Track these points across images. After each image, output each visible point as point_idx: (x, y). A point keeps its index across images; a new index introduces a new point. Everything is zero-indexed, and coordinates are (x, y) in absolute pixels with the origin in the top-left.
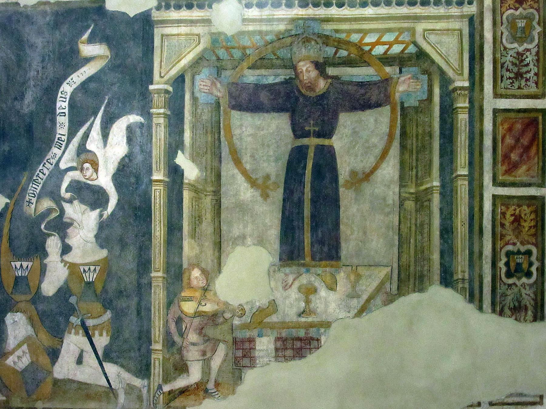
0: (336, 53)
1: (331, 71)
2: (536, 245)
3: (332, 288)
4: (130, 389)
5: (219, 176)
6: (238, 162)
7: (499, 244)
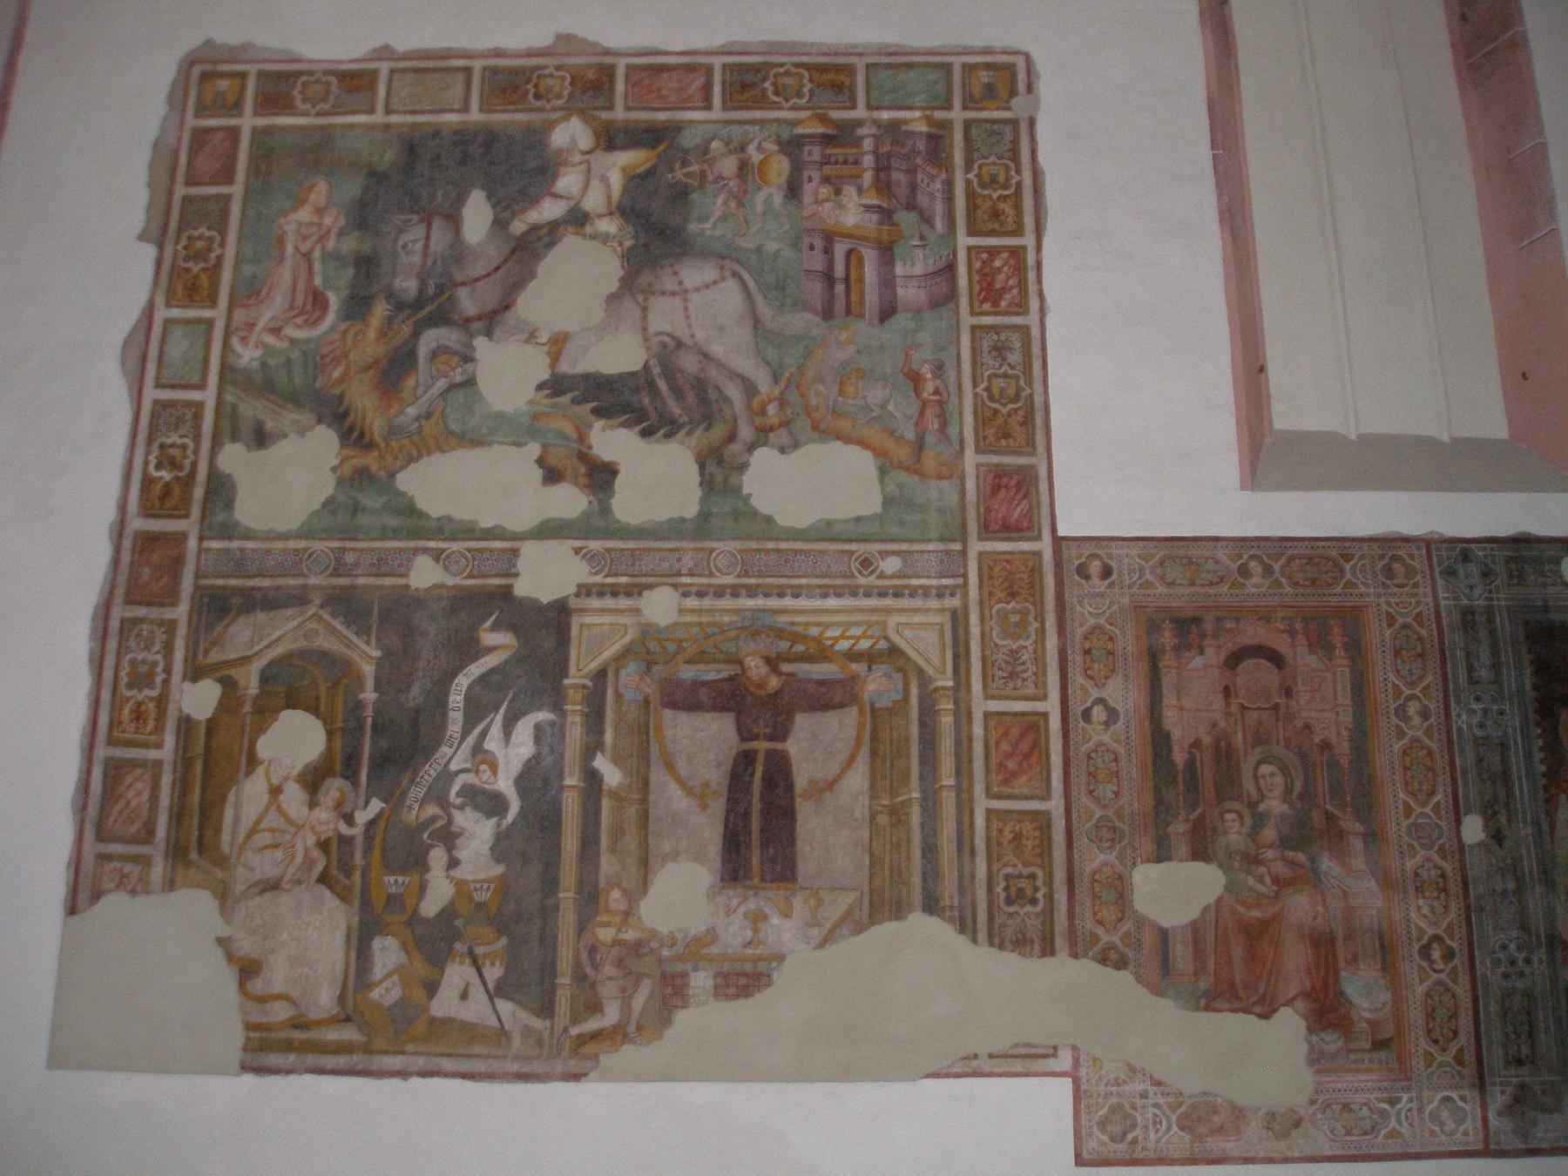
0: (791, 647)
1: (786, 668)
2: (1042, 867)
3: (786, 915)
4: (528, 1031)
5: (646, 783)
6: (670, 766)
7: (996, 865)
